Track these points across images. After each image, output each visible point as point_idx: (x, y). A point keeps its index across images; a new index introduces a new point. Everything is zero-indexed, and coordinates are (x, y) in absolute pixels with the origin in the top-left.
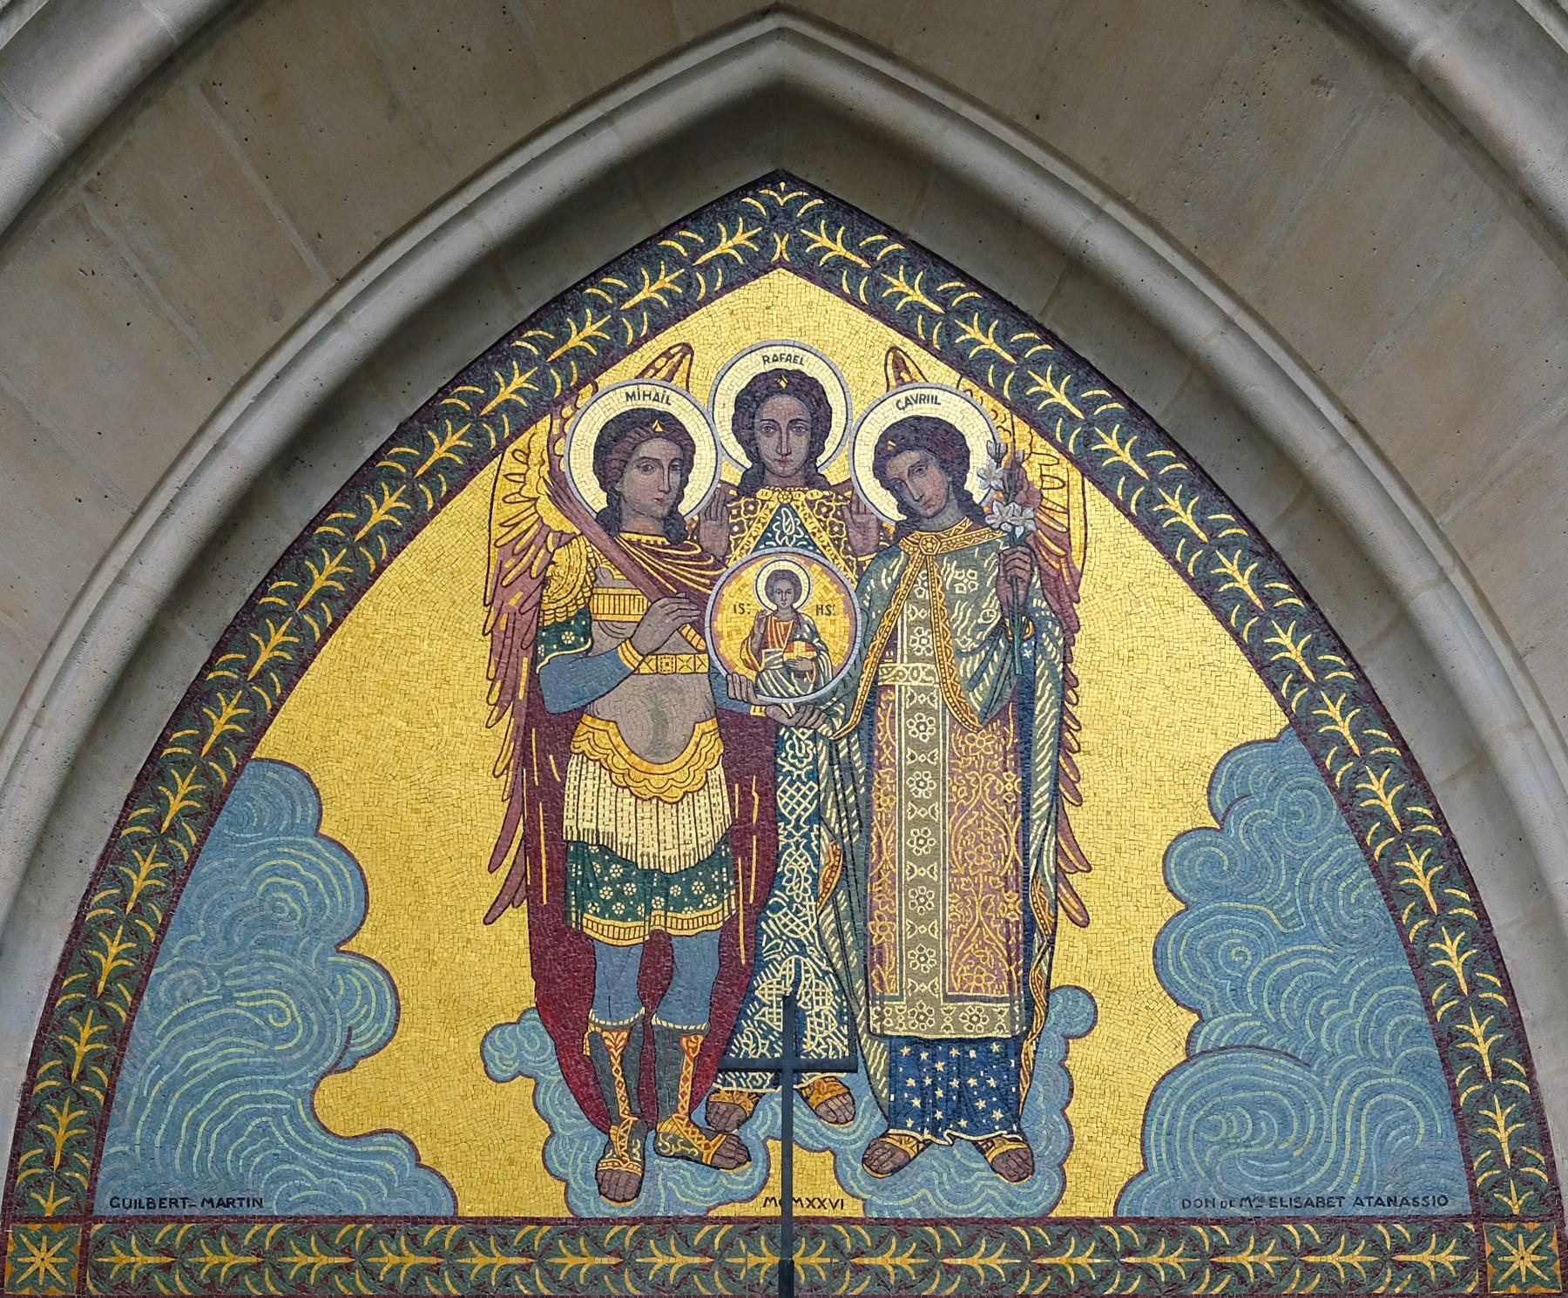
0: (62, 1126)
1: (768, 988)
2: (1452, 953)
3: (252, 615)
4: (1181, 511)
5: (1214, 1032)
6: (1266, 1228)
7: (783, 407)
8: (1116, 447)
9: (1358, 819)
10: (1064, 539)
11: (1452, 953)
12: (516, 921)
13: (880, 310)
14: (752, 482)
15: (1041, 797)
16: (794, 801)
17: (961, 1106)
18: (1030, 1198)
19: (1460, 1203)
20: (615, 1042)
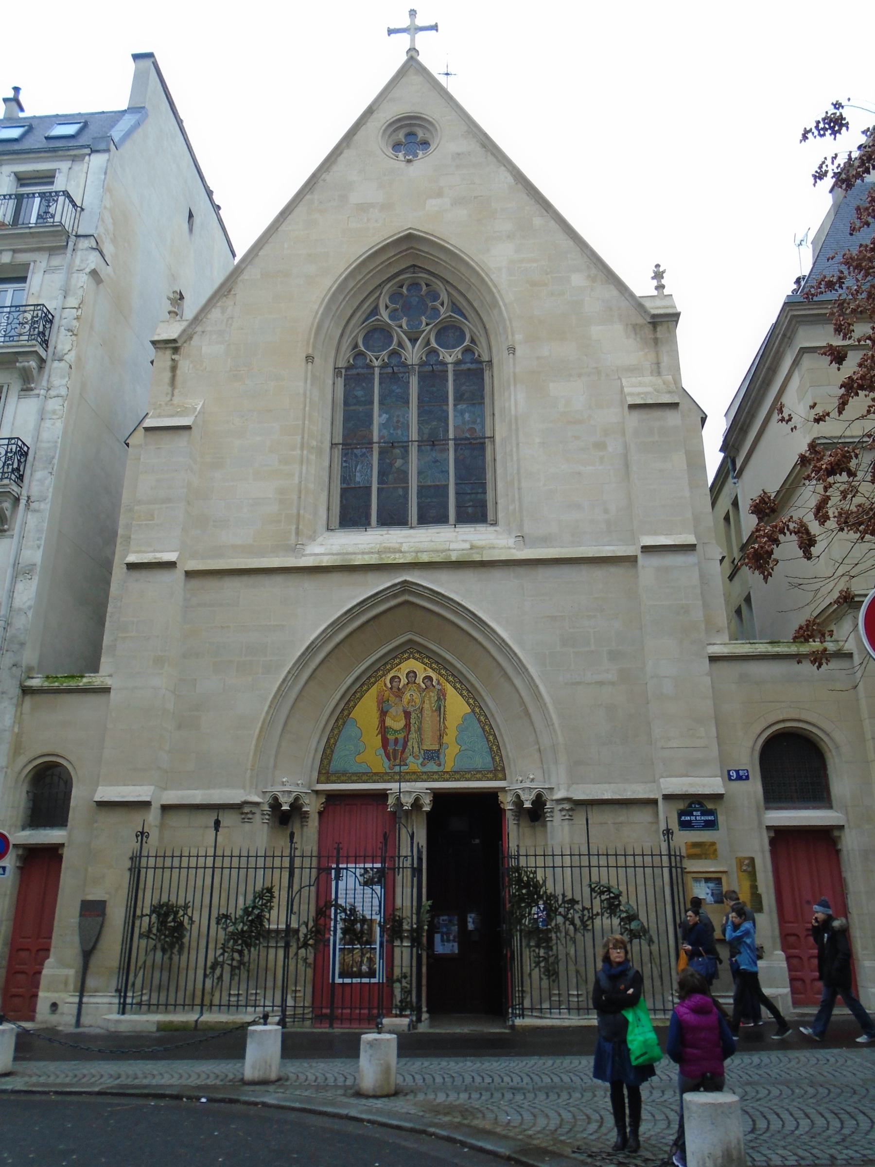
0: (325, 762)
1: (409, 744)
2: (491, 738)
3: (349, 701)
4: (458, 685)
5: (463, 748)
6: (469, 772)
7: (412, 675)
8: (451, 679)
9: (480, 721)
10: (444, 689)
11: (491, 738)
12: (380, 736)
13: (423, 663)
14: (408, 684)
15: (442, 720)
16: (412, 721)
17: (432, 758)
18: (441, 769)
19: (493, 769)
20: (391, 751)
